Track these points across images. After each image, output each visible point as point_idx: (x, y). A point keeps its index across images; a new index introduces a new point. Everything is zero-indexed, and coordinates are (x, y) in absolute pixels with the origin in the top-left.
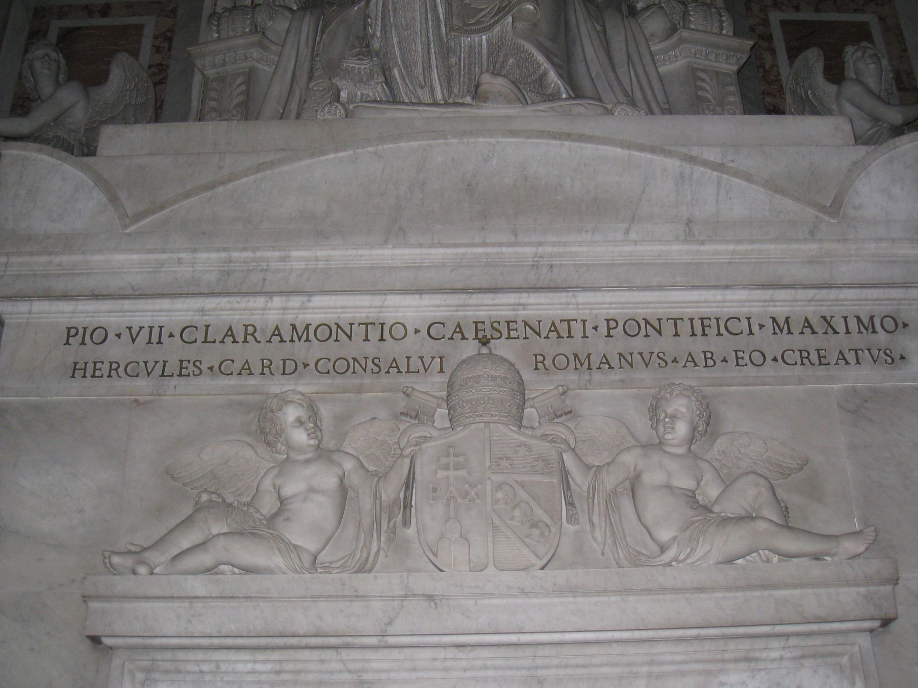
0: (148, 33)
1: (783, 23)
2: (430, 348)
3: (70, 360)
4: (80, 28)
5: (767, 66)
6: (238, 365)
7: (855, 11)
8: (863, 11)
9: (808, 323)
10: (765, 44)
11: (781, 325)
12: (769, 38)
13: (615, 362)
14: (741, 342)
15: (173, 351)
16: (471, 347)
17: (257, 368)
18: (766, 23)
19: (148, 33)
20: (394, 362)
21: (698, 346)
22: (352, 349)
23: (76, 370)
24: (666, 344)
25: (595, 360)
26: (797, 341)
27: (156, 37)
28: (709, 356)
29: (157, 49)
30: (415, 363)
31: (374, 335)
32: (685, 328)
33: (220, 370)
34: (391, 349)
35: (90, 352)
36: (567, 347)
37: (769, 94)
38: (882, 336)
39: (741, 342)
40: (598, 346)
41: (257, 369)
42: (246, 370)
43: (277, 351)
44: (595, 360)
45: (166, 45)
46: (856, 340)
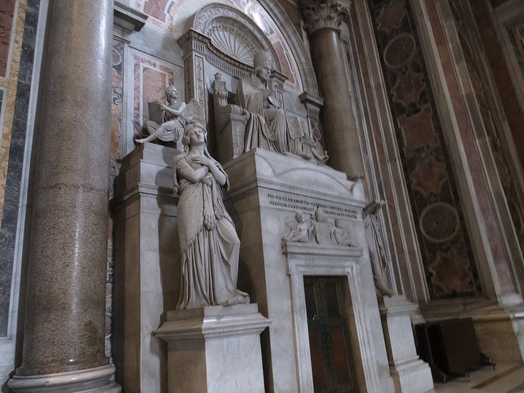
4: (149, 68)
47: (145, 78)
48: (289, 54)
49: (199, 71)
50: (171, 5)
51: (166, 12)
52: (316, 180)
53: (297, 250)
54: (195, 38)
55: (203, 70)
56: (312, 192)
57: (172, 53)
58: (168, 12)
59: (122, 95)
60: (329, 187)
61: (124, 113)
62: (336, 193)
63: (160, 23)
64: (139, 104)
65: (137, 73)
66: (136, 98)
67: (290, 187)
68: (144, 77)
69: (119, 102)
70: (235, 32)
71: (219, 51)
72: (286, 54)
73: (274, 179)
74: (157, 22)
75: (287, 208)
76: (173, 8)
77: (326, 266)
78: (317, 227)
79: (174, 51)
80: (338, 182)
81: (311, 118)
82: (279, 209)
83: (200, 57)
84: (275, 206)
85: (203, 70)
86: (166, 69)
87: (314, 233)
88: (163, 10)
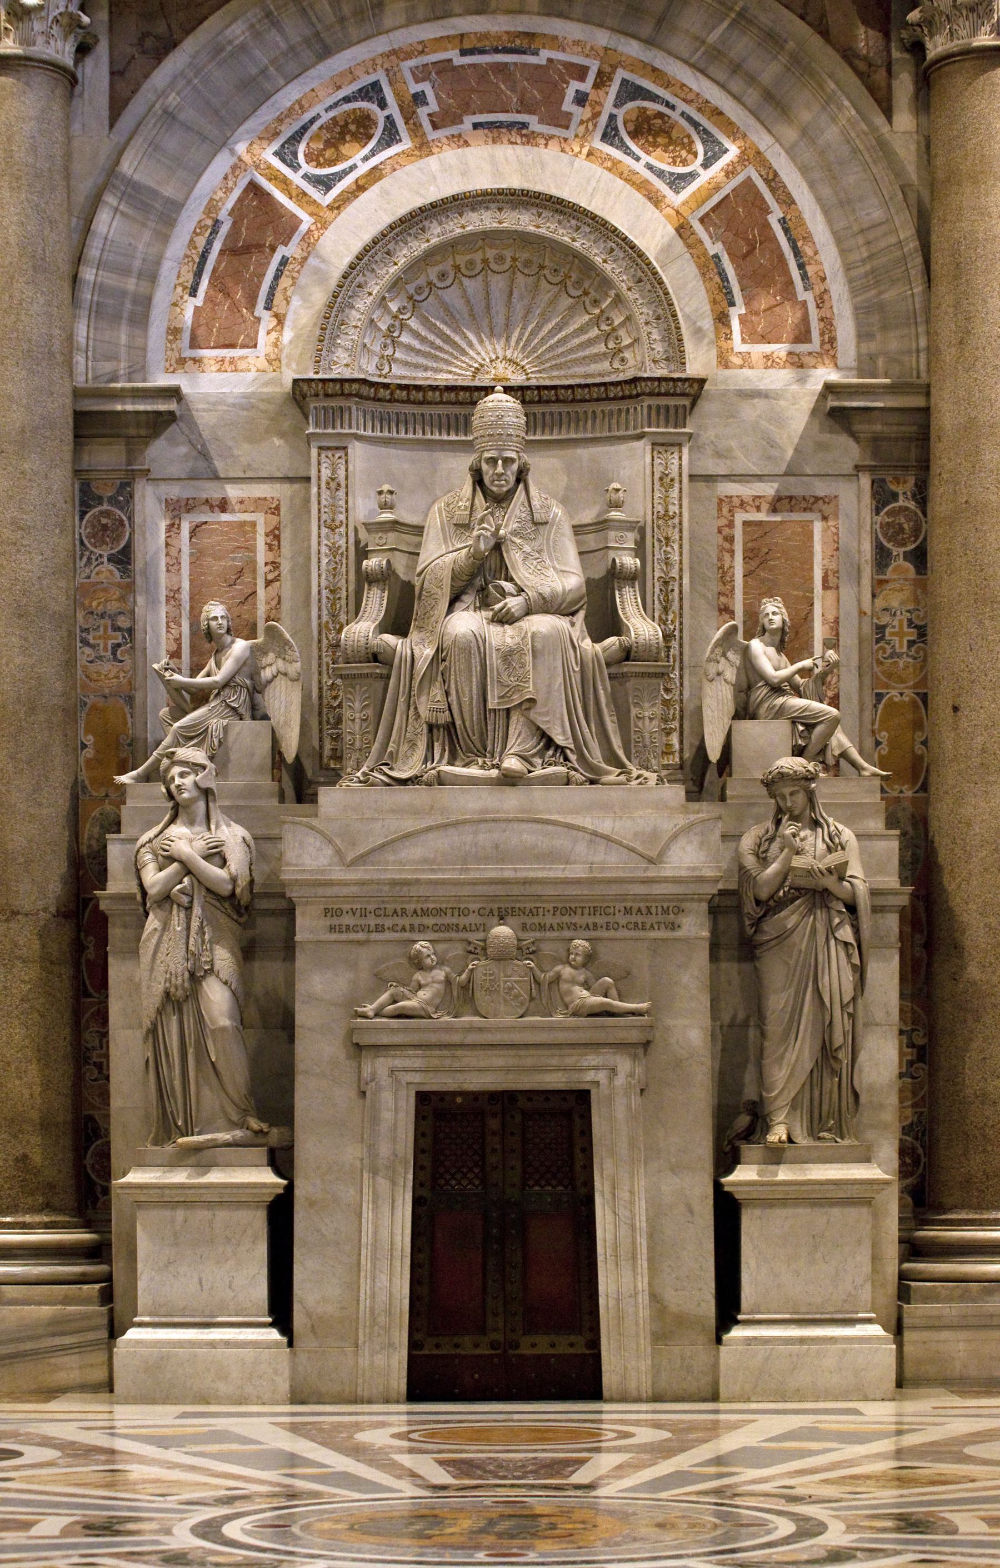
0: (261, 530)
1: (746, 523)
2: (479, 920)
3: (328, 923)
5: (726, 566)
6: (399, 928)
7: (805, 510)
8: (811, 510)
9: (639, 910)
10: (727, 545)
11: (628, 911)
12: (730, 539)
13: (555, 926)
14: (610, 919)
15: (372, 921)
16: (495, 920)
17: (408, 927)
18: (731, 524)
19: (261, 530)
20: (465, 928)
21: (590, 920)
22: (447, 920)
23: (332, 929)
24: (577, 919)
25: (548, 926)
26: (634, 918)
27: (267, 535)
28: (595, 925)
29: (270, 547)
30: (474, 928)
31: (456, 913)
32: (586, 911)
33: (393, 929)
34: (463, 921)
35: (336, 921)
36: (536, 920)
37: (724, 594)
38: (672, 916)
39: (610, 919)
40: (549, 920)
41: (408, 927)
42: (404, 929)
43: (416, 921)
44: (548, 926)
45: (275, 543)
46: (660, 918)
47: (196, 558)
48: (799, 217)
49: (333, 497)
50: (277, 277)
51: (260, 310)
52: (497, 846)
53: (385, 1040)
54: (317, 395)
55: (347, 486)
56: (474, 883)
57: (277, 442)
58: (268, 308)
59: (131, 631)
60: (552, 857)
61: (140, 673)
62: (577, 871)
63: (241, 358)
64: (178, 641)
65: (173, 552)
66: (172, 625)
67: (394, 883)
68: (191, 555)
69: (127, 651)
70: (506, 266)
71: (418, 388)
72: (783, 221)
73: (339, 874)
74: (232, 361)
75: (388, 935)
76: (285, 282)
77: (507, 1070)
78: (478, 976)
79: (282, 435)
80: (595, 834)
81: (871, 469)
82: (360, 943)
83: (337, 448)
84: (344, 937)
85: (347, 486)
86: (258, 504)
87: (467, 988)
88: (252, 304)
